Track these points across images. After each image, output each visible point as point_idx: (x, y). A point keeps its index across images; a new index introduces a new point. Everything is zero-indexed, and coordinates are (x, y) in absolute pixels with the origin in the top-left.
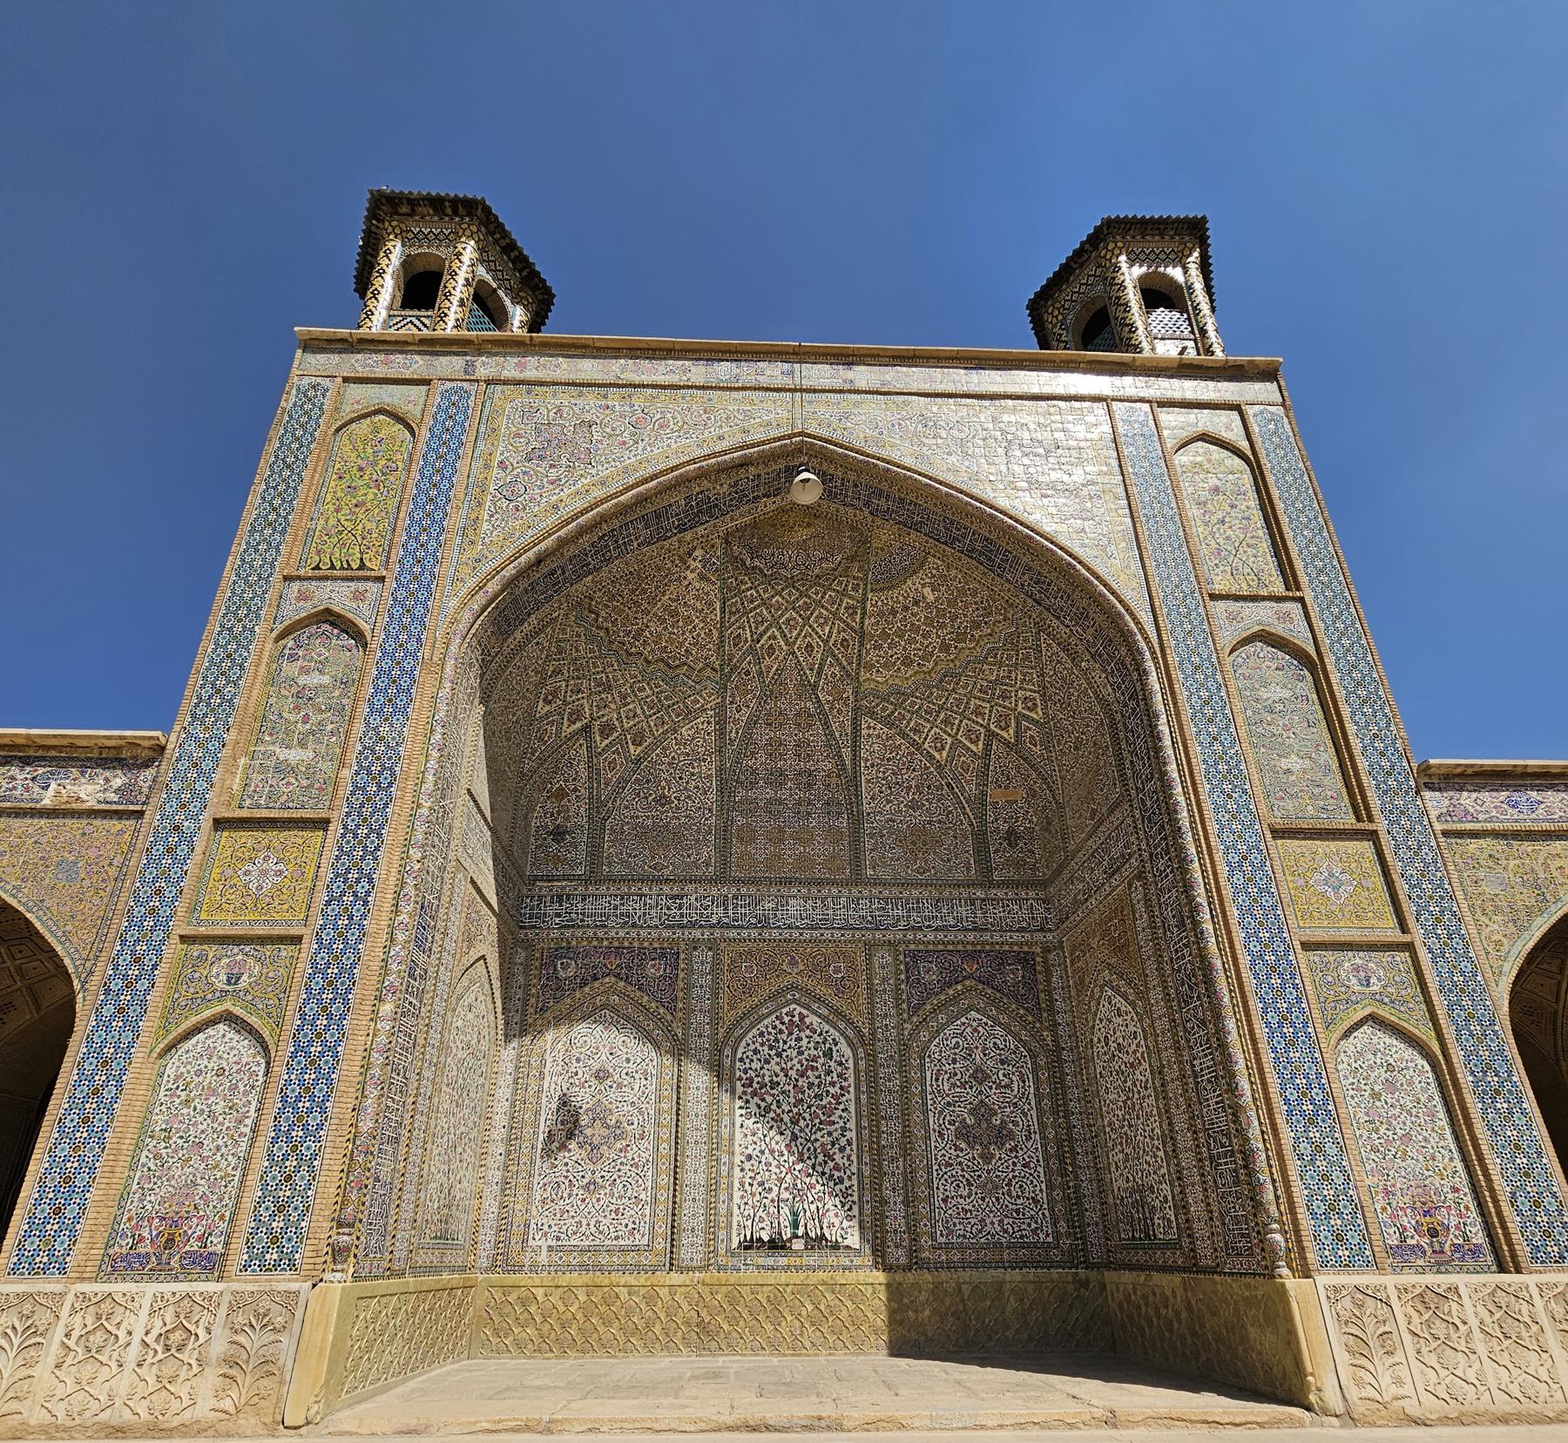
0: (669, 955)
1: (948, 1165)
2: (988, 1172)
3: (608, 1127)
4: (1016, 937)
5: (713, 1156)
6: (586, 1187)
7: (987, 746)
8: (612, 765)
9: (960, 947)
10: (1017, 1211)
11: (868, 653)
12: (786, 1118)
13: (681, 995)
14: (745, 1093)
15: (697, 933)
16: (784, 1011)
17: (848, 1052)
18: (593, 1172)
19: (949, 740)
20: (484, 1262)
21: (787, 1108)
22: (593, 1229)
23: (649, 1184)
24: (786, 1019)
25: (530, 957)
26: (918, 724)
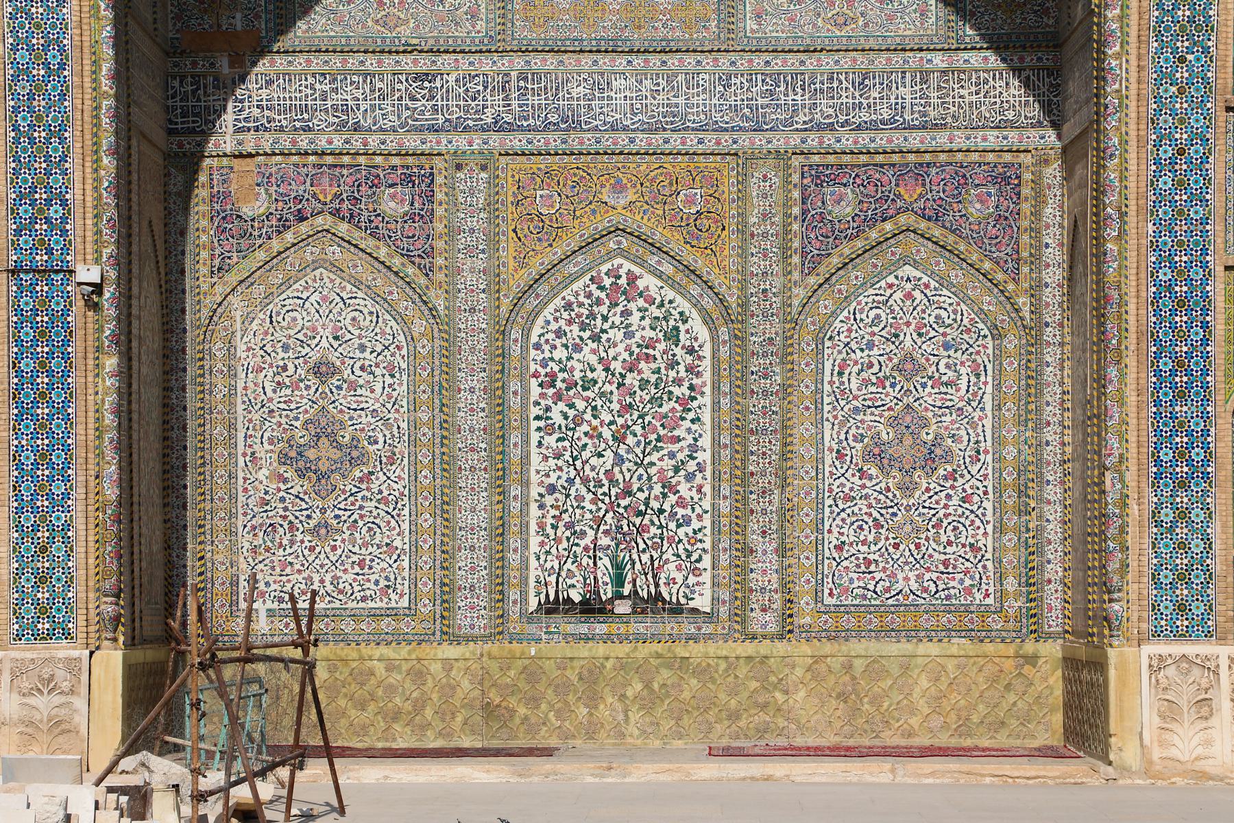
0: (417, 177)
1: (848, 498)
3: (340, 447)
4: (992, 138)
6: (314, 531)
9: (896, 158)
10: (946, 563)
12: (607, 433)
13: (440, 244)
14: (543, 395)
15: (460, 141)
16: (604, 268)
17: (703, 334)
21: (607, 418)
22: (330, 588)
23: (405, 526)
24: (607, 282)
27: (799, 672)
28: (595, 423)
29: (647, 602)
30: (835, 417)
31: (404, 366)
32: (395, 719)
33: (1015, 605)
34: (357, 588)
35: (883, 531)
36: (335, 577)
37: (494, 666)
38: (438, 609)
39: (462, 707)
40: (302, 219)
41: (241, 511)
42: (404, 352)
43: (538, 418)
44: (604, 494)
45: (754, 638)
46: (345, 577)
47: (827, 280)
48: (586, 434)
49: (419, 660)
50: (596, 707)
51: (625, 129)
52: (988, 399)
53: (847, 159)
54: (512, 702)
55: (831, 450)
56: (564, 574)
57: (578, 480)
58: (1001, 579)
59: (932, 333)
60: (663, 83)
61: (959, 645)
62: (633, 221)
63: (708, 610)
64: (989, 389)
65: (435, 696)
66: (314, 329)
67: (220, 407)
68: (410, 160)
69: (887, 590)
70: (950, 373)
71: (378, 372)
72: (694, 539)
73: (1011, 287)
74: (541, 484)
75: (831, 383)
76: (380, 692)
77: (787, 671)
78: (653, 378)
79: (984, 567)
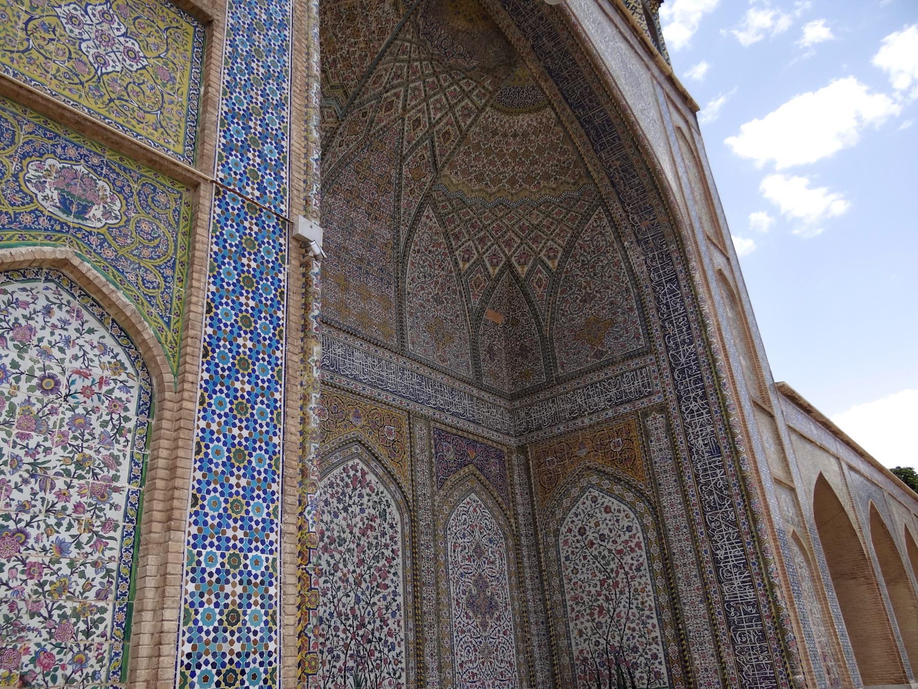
7: (502, 272)
11: (458, 155)
12: (351, 580)
16: (350, 463)
17: (397, 517)
24: (352, 473)
28: (345, 570)
44: (350, 626)
48: (340, 578)
51: (361, 381)
57: (335, 614)
62: (365, 437)
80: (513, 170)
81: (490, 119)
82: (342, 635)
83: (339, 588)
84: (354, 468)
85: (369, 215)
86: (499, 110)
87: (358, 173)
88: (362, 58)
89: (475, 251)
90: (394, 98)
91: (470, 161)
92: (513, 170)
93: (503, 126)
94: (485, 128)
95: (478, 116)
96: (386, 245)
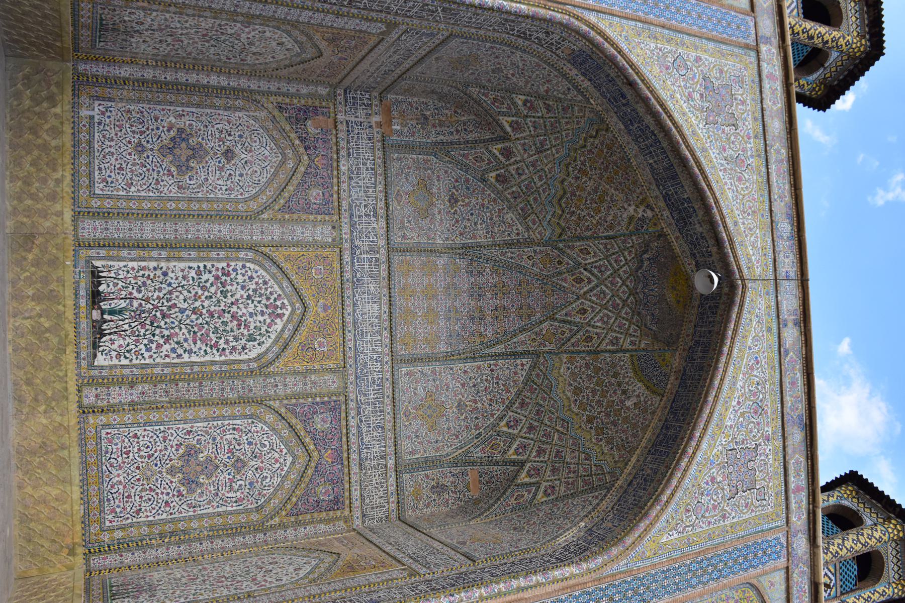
1: (165, 439)
2: (161, 472)
3: (187, 160)
4: (356, 494)
5: (164, 246)
6: (139, 144)
7: (513, 463)
8: (478, 159)
10: (129, 496)
12: (197, 304)
13: (295, 216)
14: (217, 269)
15: (346, 229)
16: (286, 301)
17: (253, 354)
18: (152, 150)
19: (516, 432)
20: (81, 67)
21: (206, 304)
22: (107, 150)
23: (143, 194)
24: (279, 303)
25: (321, 98)
26: (528, 404)
27: (58, 419)
28: (203, 297)
29: (100, 328)
30: (210, 428)
31: (232, 196)
32: (24, 182)
33: (106, 538)
34: (106, 165)
35: (146, 459)
36: (113, 154)
37: (59, 241)
38: (94, 210)
39: (33, 222)
40: (307, 148)
41: (152, 106)
42: (239, 197)
43: (205, 267)
45: (79, 391)
46: (113, 159)
47: (283, 418)
48: (197, 293)
49: (63, 198)
50: (33, 300)
51: (354, 311)
52: (224, 508)
53: (344, 423)
54: (36, 251)
55: (192, 427)
56: (116, 281)
57: (170, 288)
58: (120, 528)
59: (257, 475)
60: (376, 329)
61: (79, 510)
63: (96, 363)
64: (229, 509)
65: (39, 206)
66: (251, 151)
67: (209, 101)
68: (336, 204)
69: (111, 465)
70: (237, 487)
71: (229, 183)
72: (138, 354)
73: (284, 513)
74: (168, 268)
75: (229, 424)
76: (42, 175)
77: (59, 411)
78: (228, 328)
79: (128, 518)
80: (599, 413)
81: (622, 363)
82: (156, 294)
83: (190, 292)
84: (283, 306)
85: (496, 310)
86: (633, 363)
87: (520, 285)
88: (588, 229)
89: (519, 428)
90: (586, 281)
91: (583, 373)
92: (599, 413)
93: (624, 377)
94: (614, 365)
95: (617, 351)
96: (481, 335)
